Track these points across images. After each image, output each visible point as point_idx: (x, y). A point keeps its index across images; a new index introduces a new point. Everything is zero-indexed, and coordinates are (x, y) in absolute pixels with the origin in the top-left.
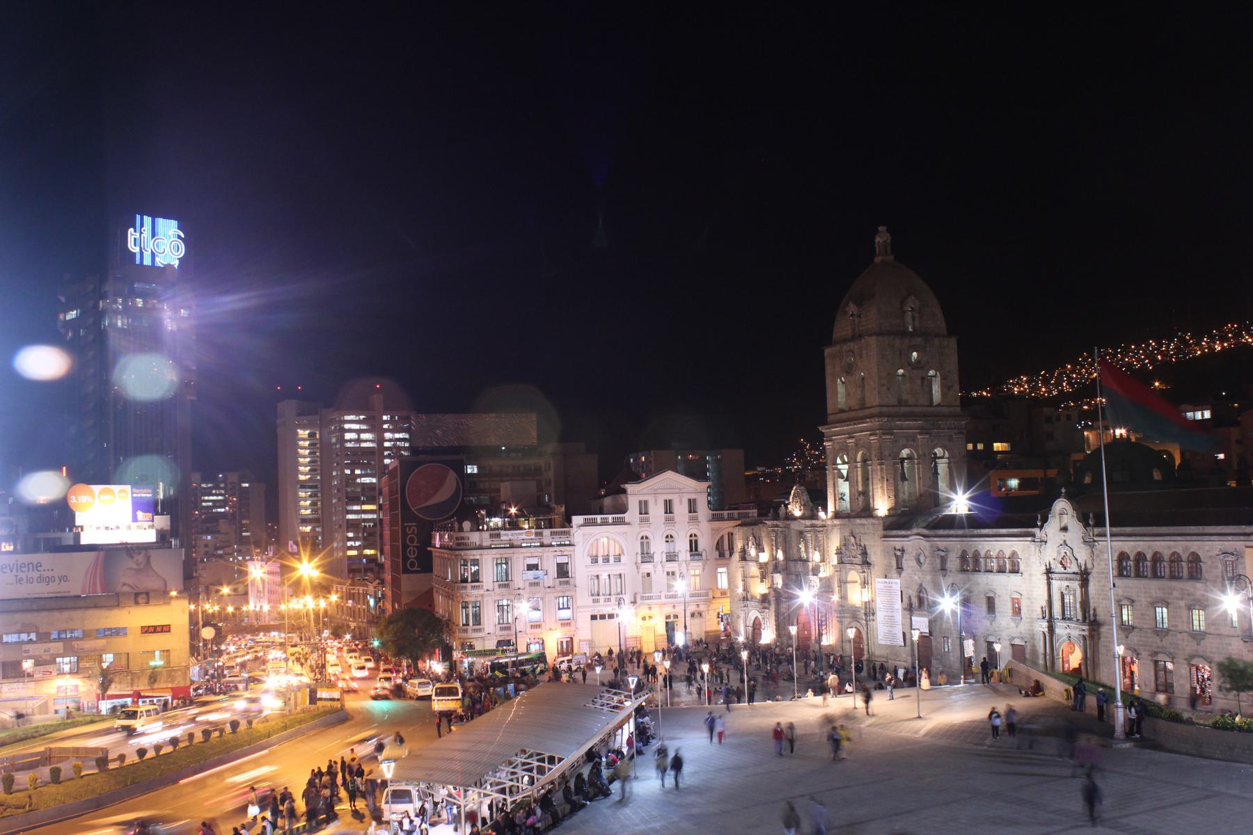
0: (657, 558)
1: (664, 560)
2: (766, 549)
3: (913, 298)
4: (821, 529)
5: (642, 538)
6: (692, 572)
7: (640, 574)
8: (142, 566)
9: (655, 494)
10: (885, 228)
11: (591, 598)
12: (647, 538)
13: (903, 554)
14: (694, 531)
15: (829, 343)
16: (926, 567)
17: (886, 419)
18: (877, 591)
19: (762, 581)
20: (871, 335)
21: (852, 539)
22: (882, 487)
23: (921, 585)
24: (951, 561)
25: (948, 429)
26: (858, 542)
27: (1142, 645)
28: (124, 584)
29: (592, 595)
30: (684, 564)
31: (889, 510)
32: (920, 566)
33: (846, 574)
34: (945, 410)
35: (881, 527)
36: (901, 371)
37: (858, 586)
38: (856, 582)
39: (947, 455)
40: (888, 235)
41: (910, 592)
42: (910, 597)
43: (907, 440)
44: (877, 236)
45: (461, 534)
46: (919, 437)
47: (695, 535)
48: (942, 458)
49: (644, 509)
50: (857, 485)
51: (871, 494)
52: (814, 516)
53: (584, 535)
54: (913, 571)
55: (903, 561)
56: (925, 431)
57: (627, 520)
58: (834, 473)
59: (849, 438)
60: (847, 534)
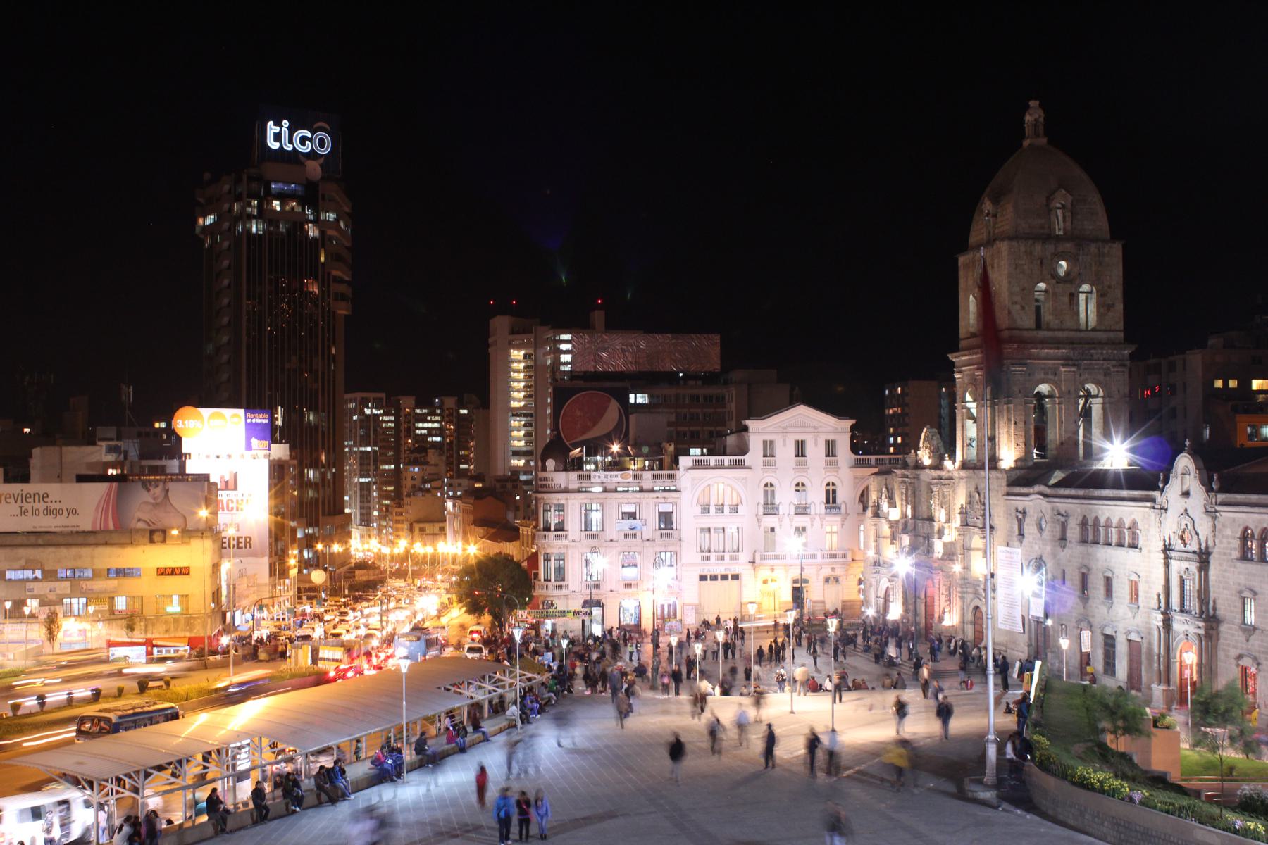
0: (782, 510)
1: (793, 512)
2: (898, 504)
3: (1064, 192)
4: (947, 482)
5: (766, 485)
6: (828, 529)
7: (762, 528)
8: (159, 501)
9: (784, 432)
10: (1038, 102)
11: (700, 555)
12: (772, 485)
13: (1024, 517)
14: (832, 479)
16: (1046, 534)
17: (1015, 346)
19: (892, 543)
20: (1003, 240)
21: (977, 495)
22: (1008, 432)
24: (1071, 529)
25: (1104, 360)
26: (982, 500)
27: (1263, 653)
28: (139, 520)
29: (702, 551)
30: (817, 518)
31: (1016, 461)
32: (1041, 533)
34: (1101, 336)
35: (1004, 483)
36: (1042, 286)
37: (980, 554)
39: (1101, 393)
40: (1041, 112)
43: (1046, 374)
44: (1027, 114)
45: (542, 475)
46: (1063, 370)
47: (833, 484)
48: (1096, 396)
49: (769, 449)
52: (938, 466)
53: (693, 479)
54: (1034, 539)
55: (1025, 527)
56: (1070, 362)
58: (962, 413)
60: (972, 489)
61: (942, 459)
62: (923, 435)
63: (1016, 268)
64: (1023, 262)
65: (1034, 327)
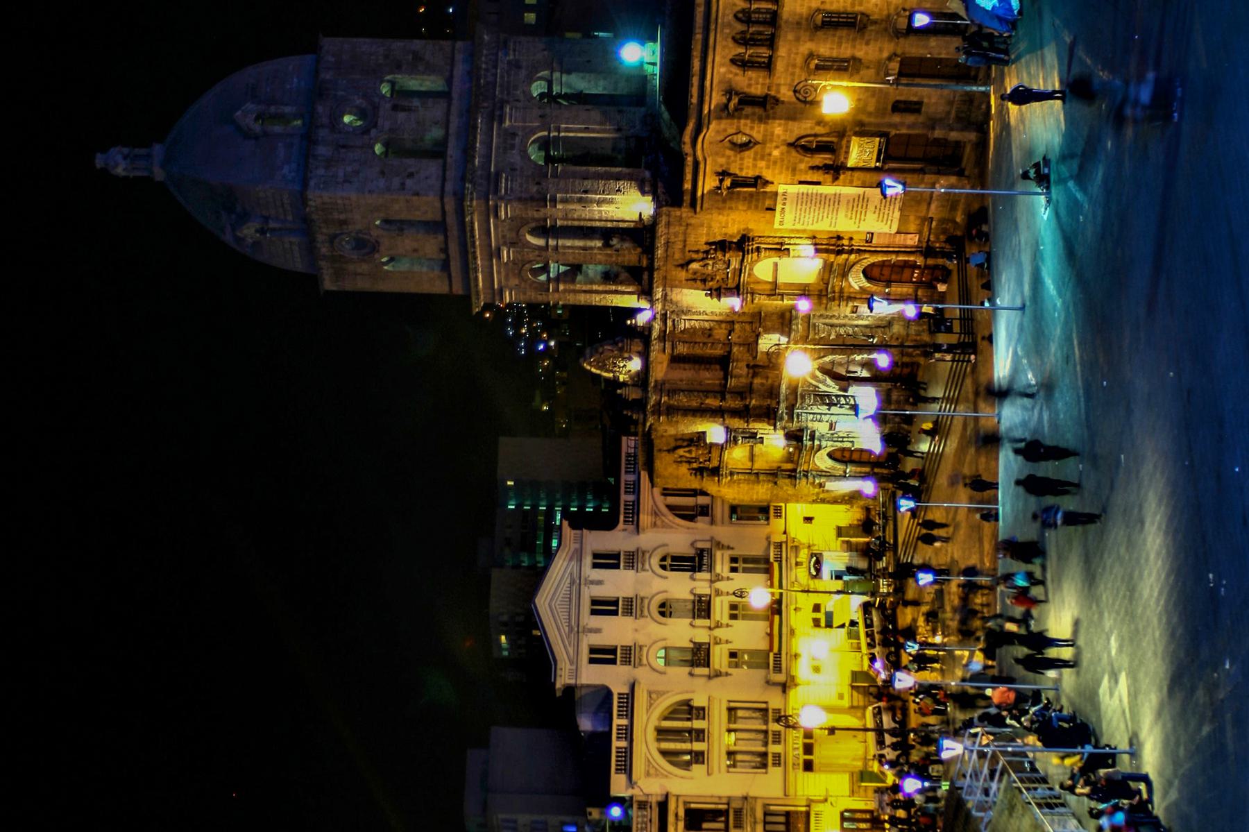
0: (702, 636)
1: (706, 622)
2: (700, 428)
3: (239, 113)
4: (669, 323)
7: (730, 671)
9: (577, 630)
10: (99, 155)
11: (771, 768)
13: (729, 175)
14: (655, 561)
15: (311, 280)
16: (757, 131)
17: (468, 185)
18: (798, 227)
19: (762, 441)
20: (304, 201)
21: (694, 266)
22: (599, 203)
23: (790, 145)
24: (750, 85)
25: (495, 67)
26: (701, 256)
29: (764, 766)
30: (719, 585)
31: (643, 193)
32: (757, 143)
33: (758, 282)
34: (460, 69)
35: (676, 212)
37: (784, 262)
38: (776, 265)
39: (545, 73)
40: (113, 151)
41: (803, 166)
42: (812, 168)
43: (513, 147)
44: (113, 172)
46: (507, 123)
47: (663, 559)
49: (603, 655)
50: (591, 248)
51: (609, 225)
52: (643, 335)
53: (648, 774)
54: (762, 158)
55: (744, 174)
56: (497, 113)
57: (626, 690)
58: (565, 291)
59: (499, 257)
60: (683, 275)
61: (634, 328)
62: (593, 370)
63: (350, 182)
64: (341, 174)
65: (441, 161)
